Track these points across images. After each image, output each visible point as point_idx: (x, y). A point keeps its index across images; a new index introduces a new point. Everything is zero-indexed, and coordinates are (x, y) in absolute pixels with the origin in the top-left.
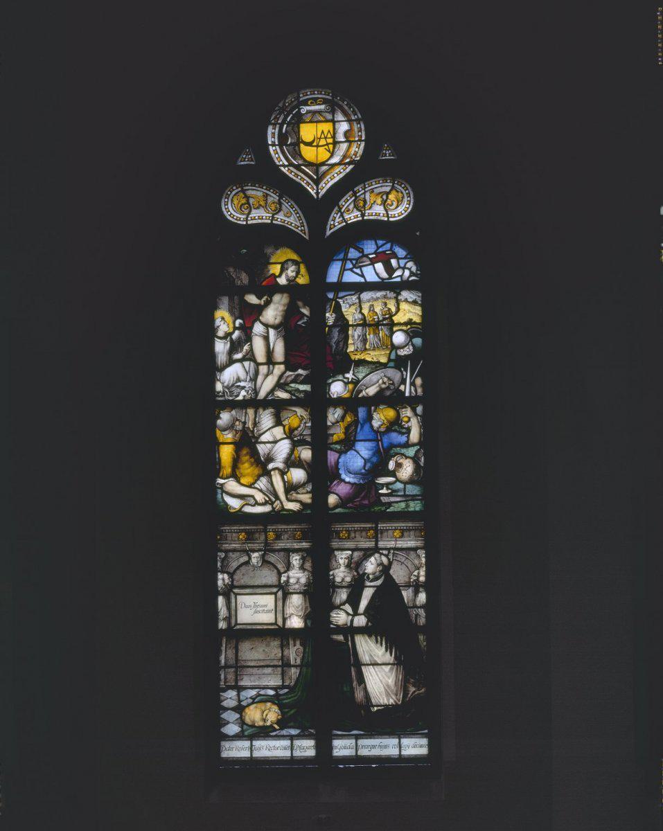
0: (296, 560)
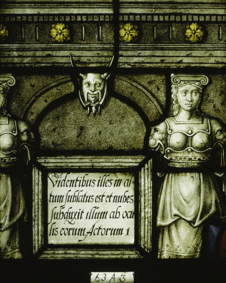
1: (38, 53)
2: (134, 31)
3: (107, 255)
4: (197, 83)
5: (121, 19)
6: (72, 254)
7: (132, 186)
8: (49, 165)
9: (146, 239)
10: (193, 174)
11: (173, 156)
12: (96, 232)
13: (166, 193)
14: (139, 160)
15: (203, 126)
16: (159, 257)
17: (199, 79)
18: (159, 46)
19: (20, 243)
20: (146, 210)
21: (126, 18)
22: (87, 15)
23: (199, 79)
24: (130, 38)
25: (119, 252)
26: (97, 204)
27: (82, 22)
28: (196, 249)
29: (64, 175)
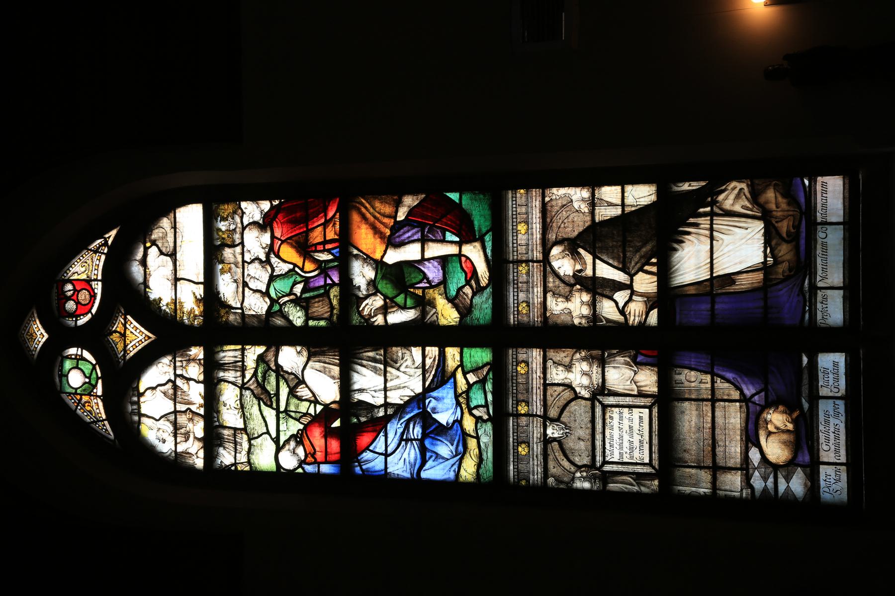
0: (557, 375)
1: (536, 463)
2: (522, 405)
3: (655, 426)
4: (552, 367)
5: (515, 413)
6: (655, 449)
7: (613, 409)
8: (600, 459)
9: (646, 402)
10: (606, 371)
11: (595, 383)
12: (641, 433)
13: (618, 388)
14: (598, 404)
15: (577, 364)
16: (657, 394)
17: (549, 367)
18: (530, 390)
19: (649, 480)
20: (628, 401)
21: (515, 409)
22: (513, 433)
23: (549, 367)
24: (526, 407)
25: (654, 419)
26: (624, 431)
27: (517, 436)
28: (652, 370)
29: (606, 450)
